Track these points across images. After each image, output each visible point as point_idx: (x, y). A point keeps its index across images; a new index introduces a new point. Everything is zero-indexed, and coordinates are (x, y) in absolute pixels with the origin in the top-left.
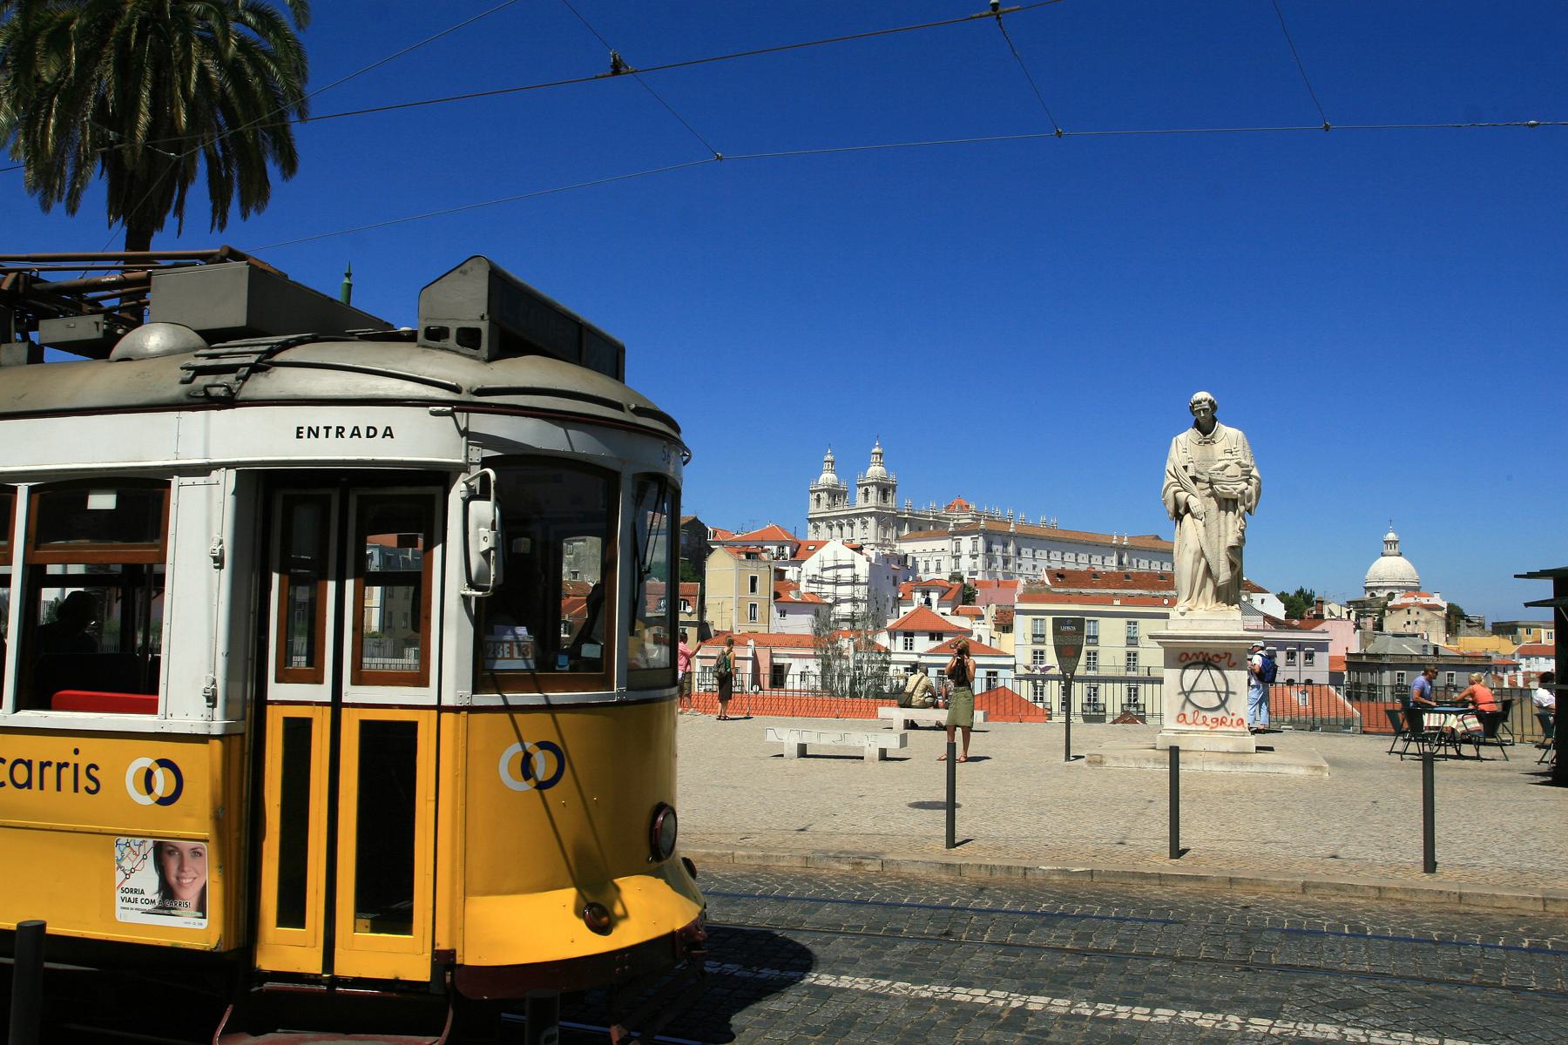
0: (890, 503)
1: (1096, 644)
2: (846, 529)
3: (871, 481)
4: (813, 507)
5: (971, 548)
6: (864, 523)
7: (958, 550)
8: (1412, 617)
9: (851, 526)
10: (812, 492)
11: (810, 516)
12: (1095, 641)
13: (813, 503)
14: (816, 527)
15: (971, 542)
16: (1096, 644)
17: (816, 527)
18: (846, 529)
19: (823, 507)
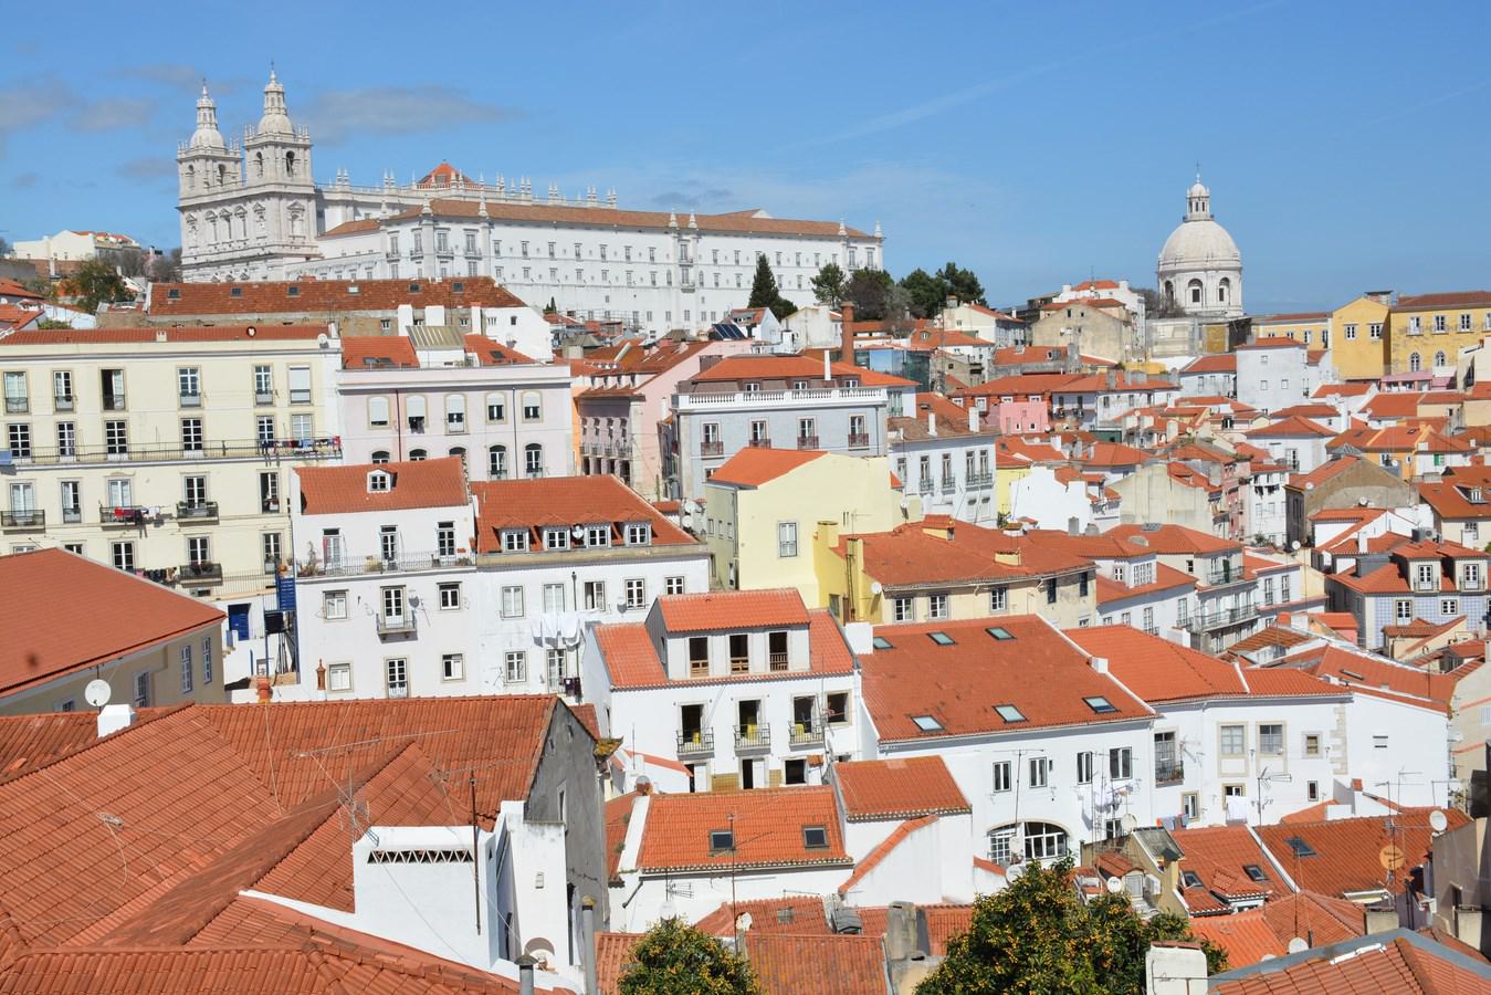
0: (302, 177)
2: (236, 221)
3: (264, 140)
4: (184, 190)
5: (413, 247)
6: (260, 211)
7: (395, 251)
8: (1075, 320)
9: (243, 216)
10: (181, 161)
11: (182, 204)
13: (184, 182)
14: (192, 221)
15: (412, 235)
17: (192, 221)
18: (236, 221)
19: (201, 189)
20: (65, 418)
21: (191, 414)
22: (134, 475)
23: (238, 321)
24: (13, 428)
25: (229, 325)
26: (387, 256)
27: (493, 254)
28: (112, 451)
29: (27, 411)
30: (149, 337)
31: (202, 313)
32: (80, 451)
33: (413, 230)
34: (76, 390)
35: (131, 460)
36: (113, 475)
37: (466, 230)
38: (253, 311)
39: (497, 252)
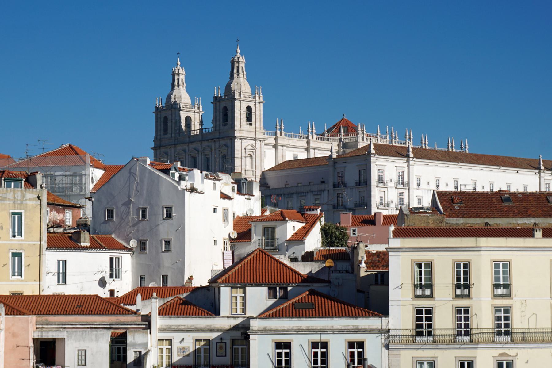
1: (509, 296)
5: (357, 179)
12: (505, 291)
16: (509, 296)
20: (463, 303)
21: (424, 303)
22: (516, 355)
23: (518, 225)
24: (419, 311)
25: (510, 226)
26: (334, 186)
27: (415, 186)
28: (499, 334)
29: (431, 296)
30: (528, 233)
31: (487, 217)
32: (437, 332)
33: (357, 166)
34: (473, 279)
35: (512, 341)
36: (501, 355)
37: (396, 166)
38: (529, 216)
39: (419, 185)
